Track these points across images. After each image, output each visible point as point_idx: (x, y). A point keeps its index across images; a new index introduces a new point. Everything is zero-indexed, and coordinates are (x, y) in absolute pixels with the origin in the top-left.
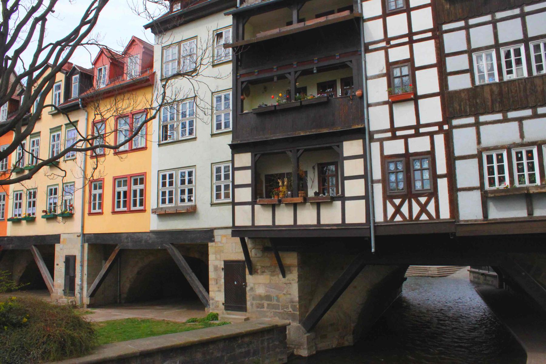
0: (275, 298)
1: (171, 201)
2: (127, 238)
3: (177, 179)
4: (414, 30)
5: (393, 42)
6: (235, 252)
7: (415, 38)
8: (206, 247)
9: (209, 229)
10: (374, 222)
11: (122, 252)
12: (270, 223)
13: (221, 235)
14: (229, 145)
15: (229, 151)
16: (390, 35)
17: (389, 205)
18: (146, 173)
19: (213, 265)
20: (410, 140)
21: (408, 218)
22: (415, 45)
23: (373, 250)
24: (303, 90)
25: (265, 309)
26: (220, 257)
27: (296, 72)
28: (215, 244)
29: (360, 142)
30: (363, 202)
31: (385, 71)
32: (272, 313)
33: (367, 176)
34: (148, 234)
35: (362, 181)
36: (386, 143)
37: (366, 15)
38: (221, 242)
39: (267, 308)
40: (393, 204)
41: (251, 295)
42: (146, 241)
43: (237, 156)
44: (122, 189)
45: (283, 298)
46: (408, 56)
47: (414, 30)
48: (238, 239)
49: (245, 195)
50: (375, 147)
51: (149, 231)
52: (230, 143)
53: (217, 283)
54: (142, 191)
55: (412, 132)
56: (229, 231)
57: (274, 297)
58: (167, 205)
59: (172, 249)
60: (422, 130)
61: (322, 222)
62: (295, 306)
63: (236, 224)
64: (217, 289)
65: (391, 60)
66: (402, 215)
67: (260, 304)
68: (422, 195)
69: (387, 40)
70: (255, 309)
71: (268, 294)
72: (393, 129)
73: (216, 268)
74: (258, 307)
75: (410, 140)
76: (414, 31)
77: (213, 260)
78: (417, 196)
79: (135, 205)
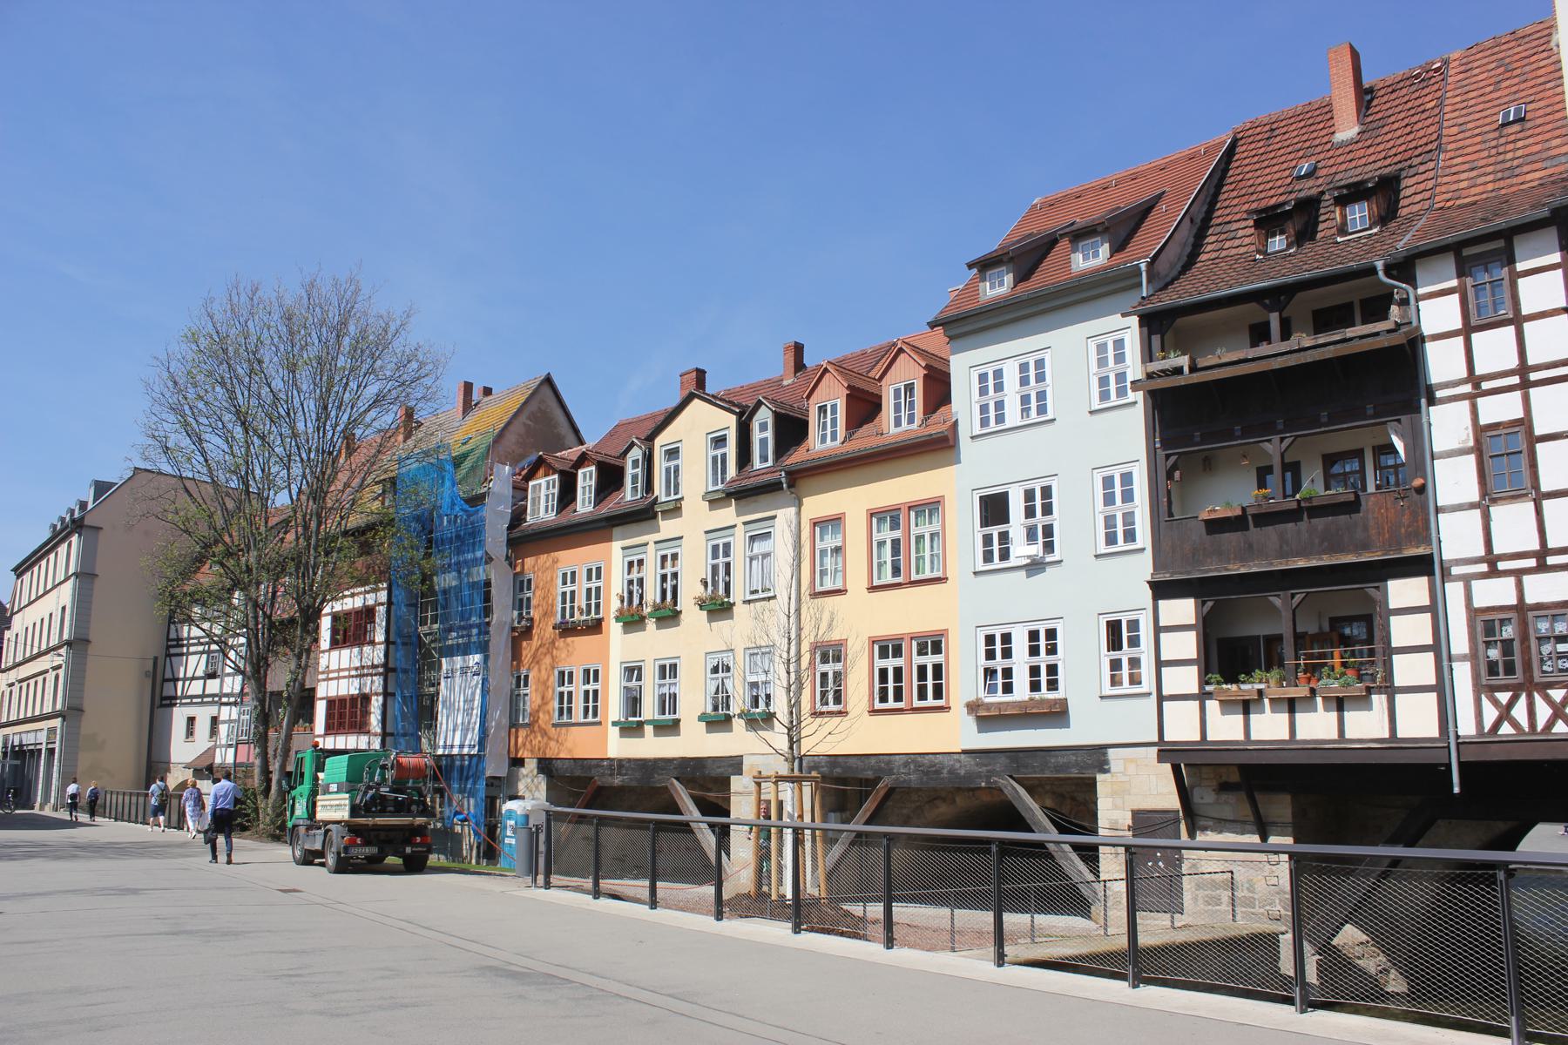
0: (1246, 885)
1: (1008, 688)
2: (906, 764)
3: (1020, 644)
4: (1531, 361)
5: (1485, 386)
7: (1534, 376)
8: (1091, 785)
10: (1458, 737)
11: (891, 792)
12: (1240, 736)
14: (1148, 582)
15: (1150, 592)
16: (1479, 371)
17: (1486, 703)
18: (947, 630)
20: (1526, 579)
21: (1527, 730)
22: (1532, 391)
23: (1456, 790)
24: (1293, 469)
27: (1282, 440)
29: (1424, 580)
30: (1433, 696)
31: (1471, 443)
33: (1438, 646)
34: (956, 757)
35: (1430, 656)
36: (1475, 584)
37: (1427, 329)
38: (1124, 773)
40: (1496, 702)
42: (952, 771)
43: (1161, 602)
44: (891, 663)
45: (1260, 886)
46: (1520, 414)
47: (1531, 361)
48: (1168, 767)
49: (1185, 680)
50: (1454, 591)
52: (1149, 579)
54: (938, 669)
55: (1532, 563)
56: (1155, 750)
58: (1000, 697)
59: (1014, 788)
60: (1551, 560)
61: (1348, 735)
63: (1167, 738)
65: (1483, 421)
66: (1515, 724)
67: (1212, 897)
68: (1551, 685)
69: (1473, 378)
72: (1491, 559)
75: (1526, 579)
76: (1530, 362)
78: (1544, 688)
79: (922, 696)
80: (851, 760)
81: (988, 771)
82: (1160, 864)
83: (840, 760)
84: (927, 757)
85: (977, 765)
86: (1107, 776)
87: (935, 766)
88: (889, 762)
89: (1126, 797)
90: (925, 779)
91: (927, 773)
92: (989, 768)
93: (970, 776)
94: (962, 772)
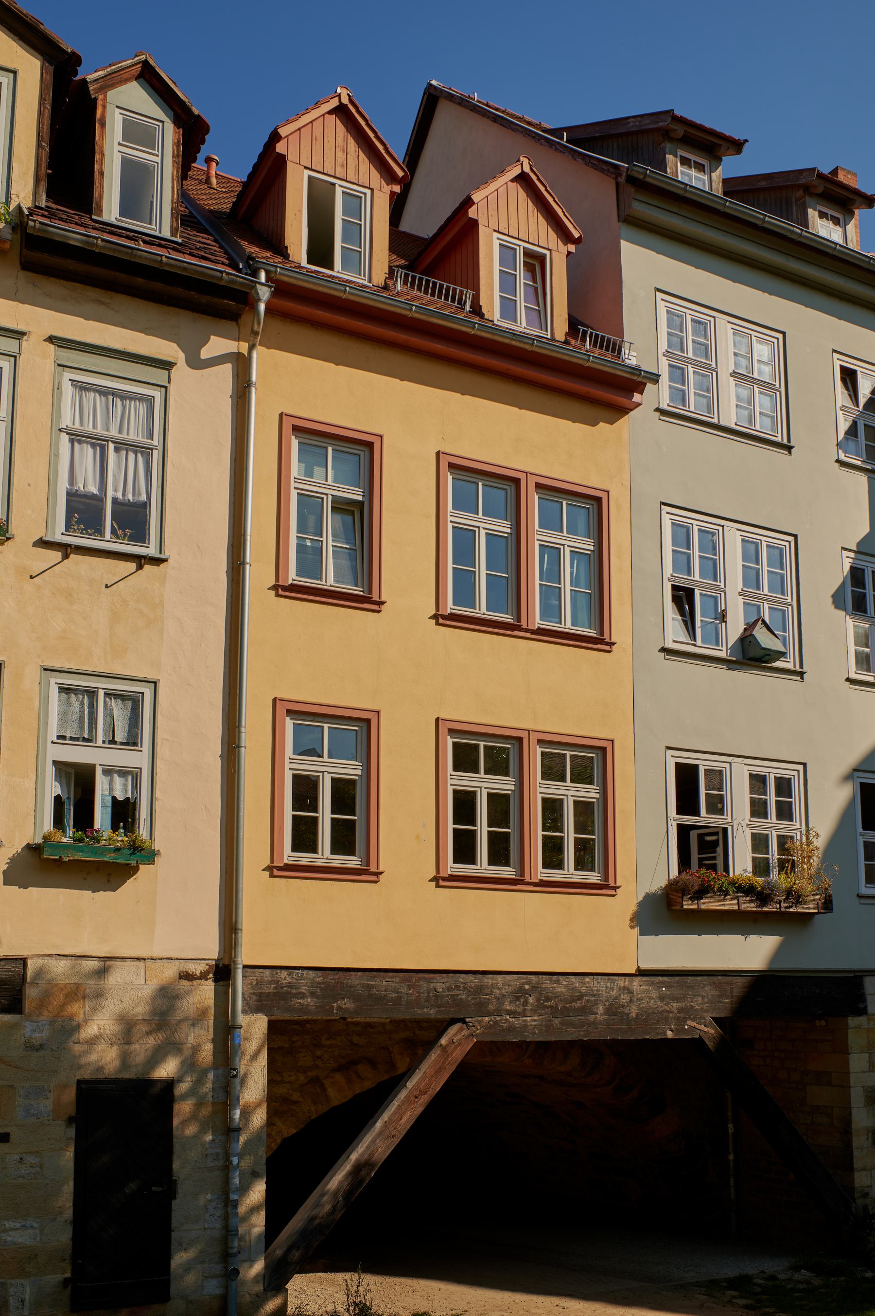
2: (519, 994)
9: (852, 975)
28: (869, 1019)
42: (613, 1010)
80: (383, 984)
81: (681, 1010)
83: (354, 980)
84: (564, 981)
85: (662, 998)
86: (862, 1020)
87: (580, 998)
88: (480, 990)
91: (565, 1012)
93: (646, 1018)
94: (634, 1011)
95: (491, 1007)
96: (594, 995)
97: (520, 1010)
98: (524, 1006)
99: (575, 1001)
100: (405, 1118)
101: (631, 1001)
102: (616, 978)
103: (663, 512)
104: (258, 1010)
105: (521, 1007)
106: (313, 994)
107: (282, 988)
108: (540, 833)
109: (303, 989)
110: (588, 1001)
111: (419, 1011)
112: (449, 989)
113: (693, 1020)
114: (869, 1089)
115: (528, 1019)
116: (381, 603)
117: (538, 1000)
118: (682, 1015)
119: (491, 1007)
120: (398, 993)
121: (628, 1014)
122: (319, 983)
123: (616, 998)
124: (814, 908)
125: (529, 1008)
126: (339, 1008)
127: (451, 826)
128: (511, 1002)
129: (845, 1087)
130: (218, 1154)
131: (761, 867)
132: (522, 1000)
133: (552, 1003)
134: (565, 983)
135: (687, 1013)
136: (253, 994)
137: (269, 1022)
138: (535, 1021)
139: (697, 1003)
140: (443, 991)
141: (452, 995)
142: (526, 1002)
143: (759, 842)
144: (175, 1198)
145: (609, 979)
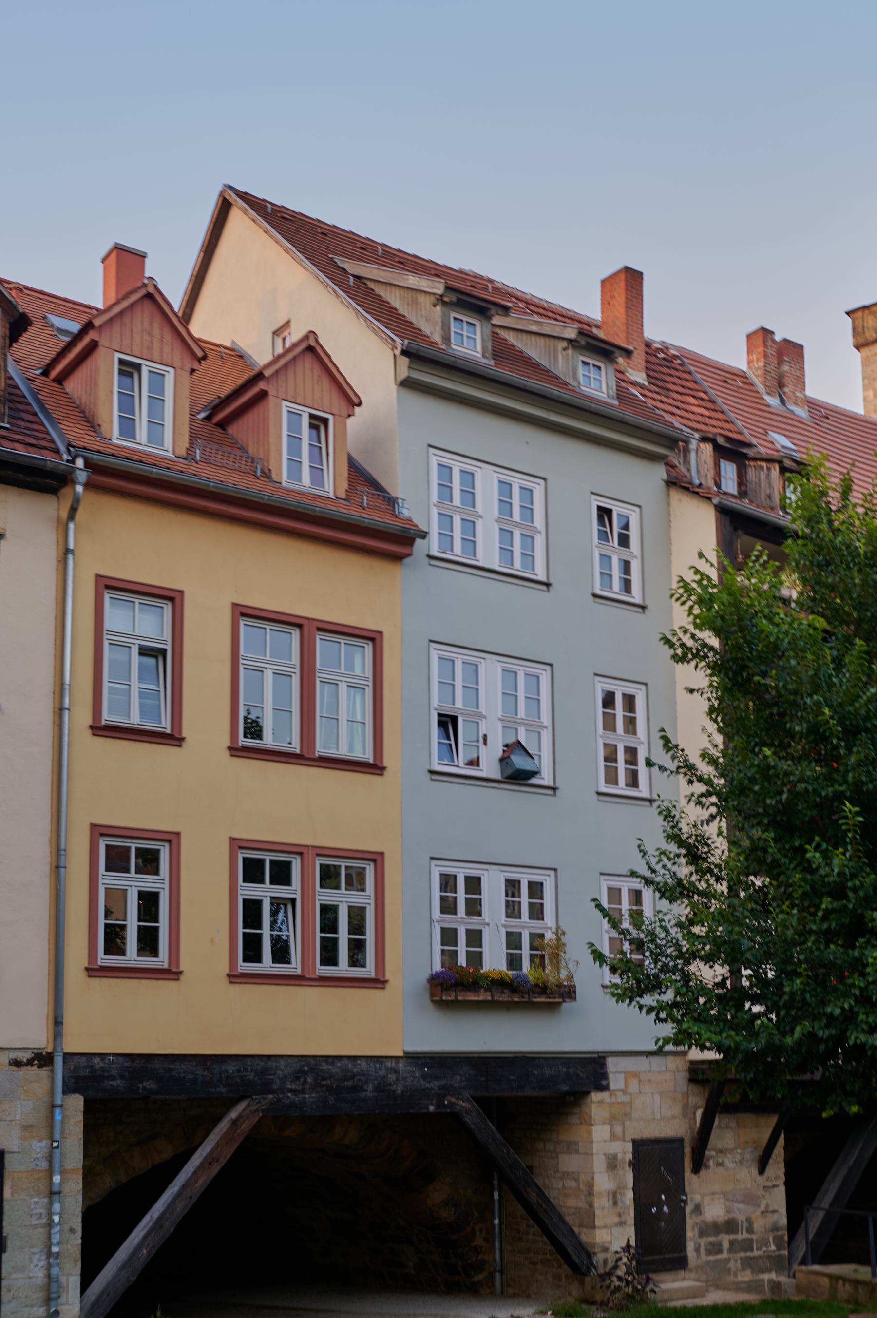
0: (745, 1225)
2: (299, 1075)
6: (659, 1117)
9: (596, 1056)
13: (625, 1073)
19: (605, 1154)
25: (725, 1255)
26: (624, 1132)
28: (611, 1095)
32: (739, 1261)
38: (624, 1092)
39: (730, 1250)
41: (697, 1224)
42: (382, 1088)
45: (759, 1225)
51: (401, 1054)
53: (615, 1203)
57: (742, 1222)
62: (782, 1236)
64: (616, 1219)
67: (712, 1244)
70: (704, 1257)
71: (731, 1216)
73: (612, 1163)
74: (709, 1252)
77: (605, 1141)
79: (329, 957)
81: (441, 1088)
82: (665, 1209)
83: (157, 1065)
85: (424, 1077)
86: (605, 1095)
87: (352, 1077)
89: (628, 1123)
90: (331, 1100)
92: (443, 1082)
94: (399, 1089)
95: (275, 1086)
96: (364, 1075)
97: (299, 1088)
98: (303, 1085)
99: (348, 1080)
100: (200, 1181)
101: (397, 1079)
102: (384, 1060)
103: (432, 650)
104: (75, 1091)
105: (301, 1086)
106: (122, 1077)
107: (96, 1071)
108: (318, 934)
109: (114, 1073)
110: (359, 1080)
111: (213, 1090)
112: (239, 1071)
113: (452, 1096)
114: (611, 1157)
115: (307, 1096)
116: (183, 739)
117: (315, 1079)
118: (442, 1092)
119: (275, 1086)
120: (195, 1074)
121: (394, 1092)
122: (128, 1067)
123: (384, 1077)
124: (559, 998)
125: (308, 1086)
126: (144, 1088)
127: (241, 930)
128: (292, 1081)
129: (589, 1154)
130: (41, 1214)
131: (514, 962)
132: (302, 1080)
133: (329, 1082)
134: (339, 1065)
135: (447, 1090)
136: (72, 1077)
137: (85, 1101)
138: (313, 1097)
139: (457, 1081)
140: (233, 1073)
141: (241, 1077)
142: (305, 1082)
143: (513, 940)
144: (5, 1251)
145: (377, 1061)
